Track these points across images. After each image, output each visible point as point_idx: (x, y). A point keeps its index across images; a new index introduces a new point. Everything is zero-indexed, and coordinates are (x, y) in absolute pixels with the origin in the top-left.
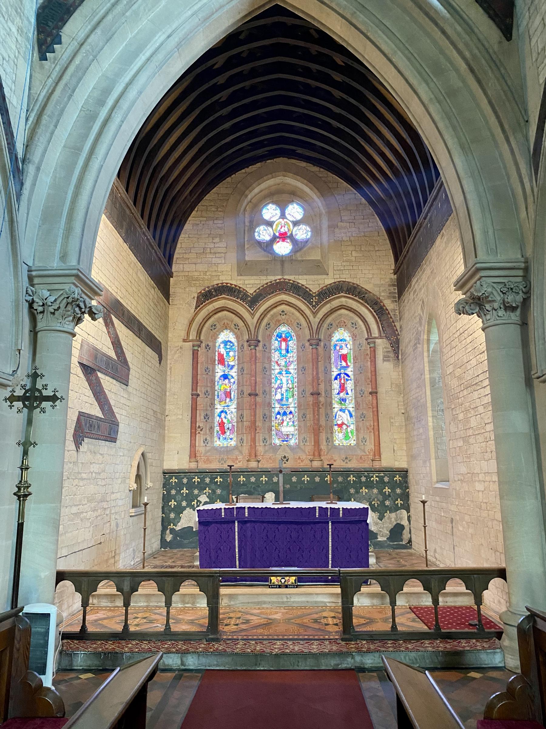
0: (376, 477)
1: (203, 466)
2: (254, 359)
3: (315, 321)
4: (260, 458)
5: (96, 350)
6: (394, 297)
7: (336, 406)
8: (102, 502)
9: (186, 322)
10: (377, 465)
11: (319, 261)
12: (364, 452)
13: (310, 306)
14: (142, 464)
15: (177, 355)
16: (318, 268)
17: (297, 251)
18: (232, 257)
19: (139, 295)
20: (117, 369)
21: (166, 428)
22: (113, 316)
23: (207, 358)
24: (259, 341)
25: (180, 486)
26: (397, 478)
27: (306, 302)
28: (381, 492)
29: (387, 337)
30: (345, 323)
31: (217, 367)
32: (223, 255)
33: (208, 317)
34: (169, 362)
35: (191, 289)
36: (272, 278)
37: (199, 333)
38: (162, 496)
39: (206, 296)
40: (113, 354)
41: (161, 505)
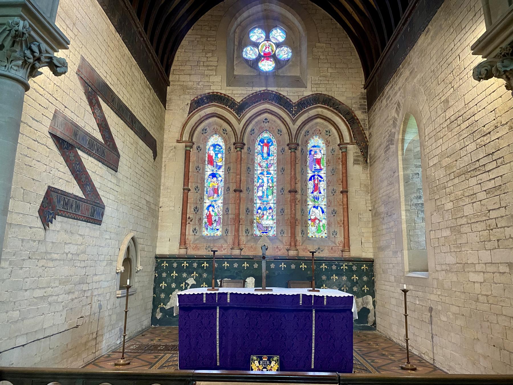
0: (346, 265)
1: (191, 252)
2: (240, 160)
3: (294, 128)
4: (242, 246)
5: (77, 126)
6: (365, 109)
7: (310, 203)
8: (79, 284)
9: (180, 125)
10: (346, 255)
12: (335, 243)
13: (291, 115)
14: (132, 248)
15: (171, 154)
16: (297, 82)
17: (279, 69)
18: (223, 68)
19: (133, 89)
20: (104, 152)
21: (159, 218)
22: (100, 99)
23: (198, 158)
24: (244, 144)
25: (170, 269)
26: (364, 267)
27: (286, 111)
28: (349, 279)
29: (357, 143)
30: (320, 131)
31: (206, 167)
32: (214, 68)
33: (199, 122)
34: (163, 160)
35: (186, 96)
36: (257, 89)
37: (192, 135)
38: (153, 278)
39: (197, 104)
40: (99, 137)
41: (152, 287)
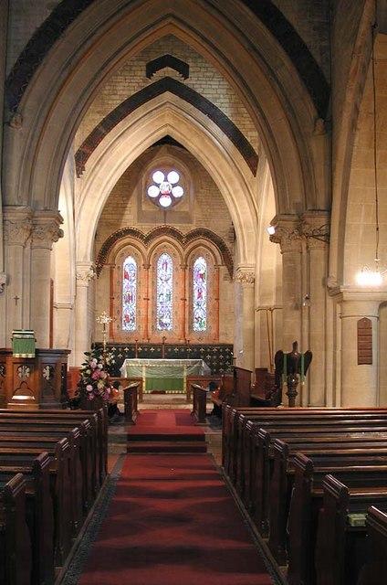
1: (116, 341)
10: (217, 342)
11: (187, 213)
16: (187, 218)
